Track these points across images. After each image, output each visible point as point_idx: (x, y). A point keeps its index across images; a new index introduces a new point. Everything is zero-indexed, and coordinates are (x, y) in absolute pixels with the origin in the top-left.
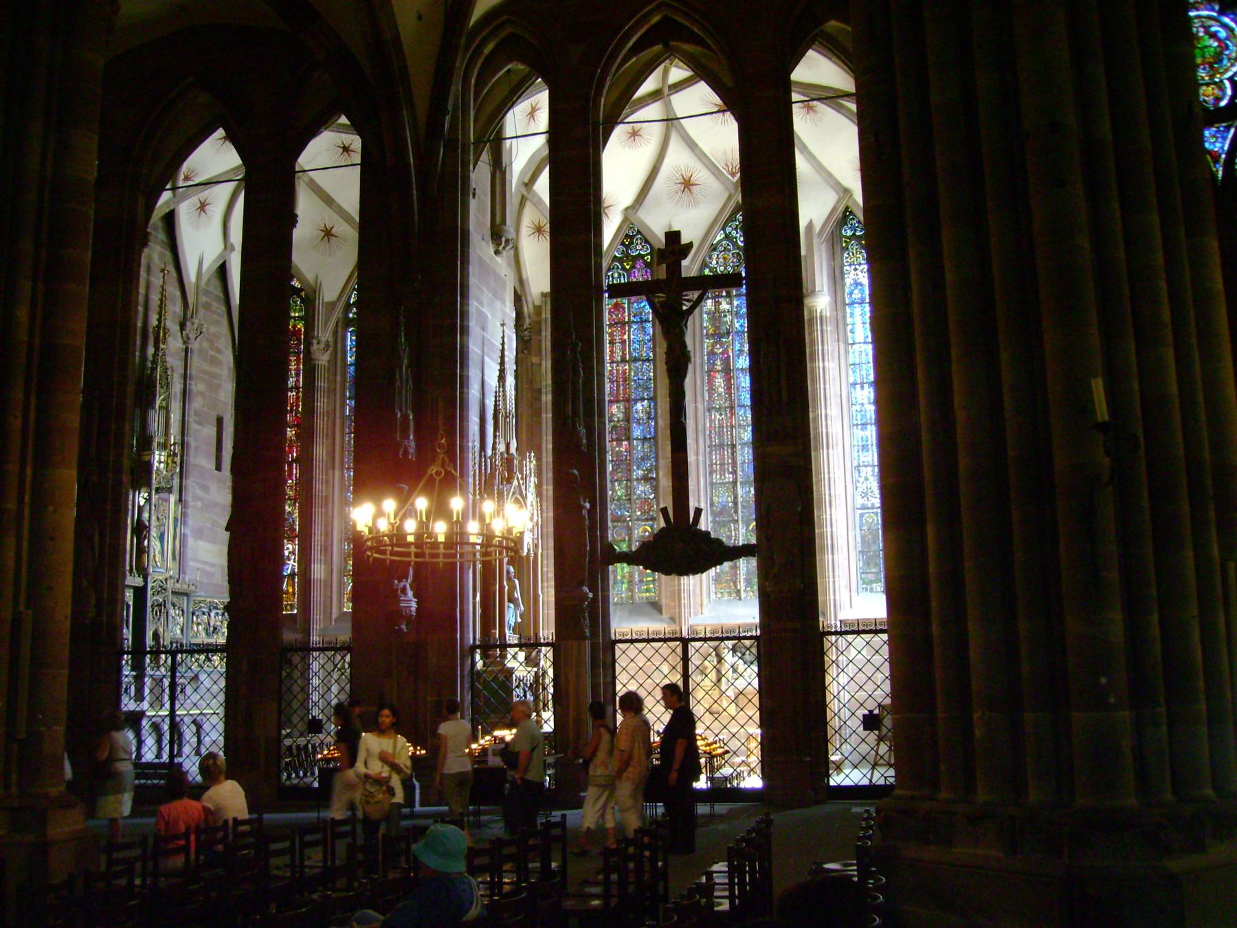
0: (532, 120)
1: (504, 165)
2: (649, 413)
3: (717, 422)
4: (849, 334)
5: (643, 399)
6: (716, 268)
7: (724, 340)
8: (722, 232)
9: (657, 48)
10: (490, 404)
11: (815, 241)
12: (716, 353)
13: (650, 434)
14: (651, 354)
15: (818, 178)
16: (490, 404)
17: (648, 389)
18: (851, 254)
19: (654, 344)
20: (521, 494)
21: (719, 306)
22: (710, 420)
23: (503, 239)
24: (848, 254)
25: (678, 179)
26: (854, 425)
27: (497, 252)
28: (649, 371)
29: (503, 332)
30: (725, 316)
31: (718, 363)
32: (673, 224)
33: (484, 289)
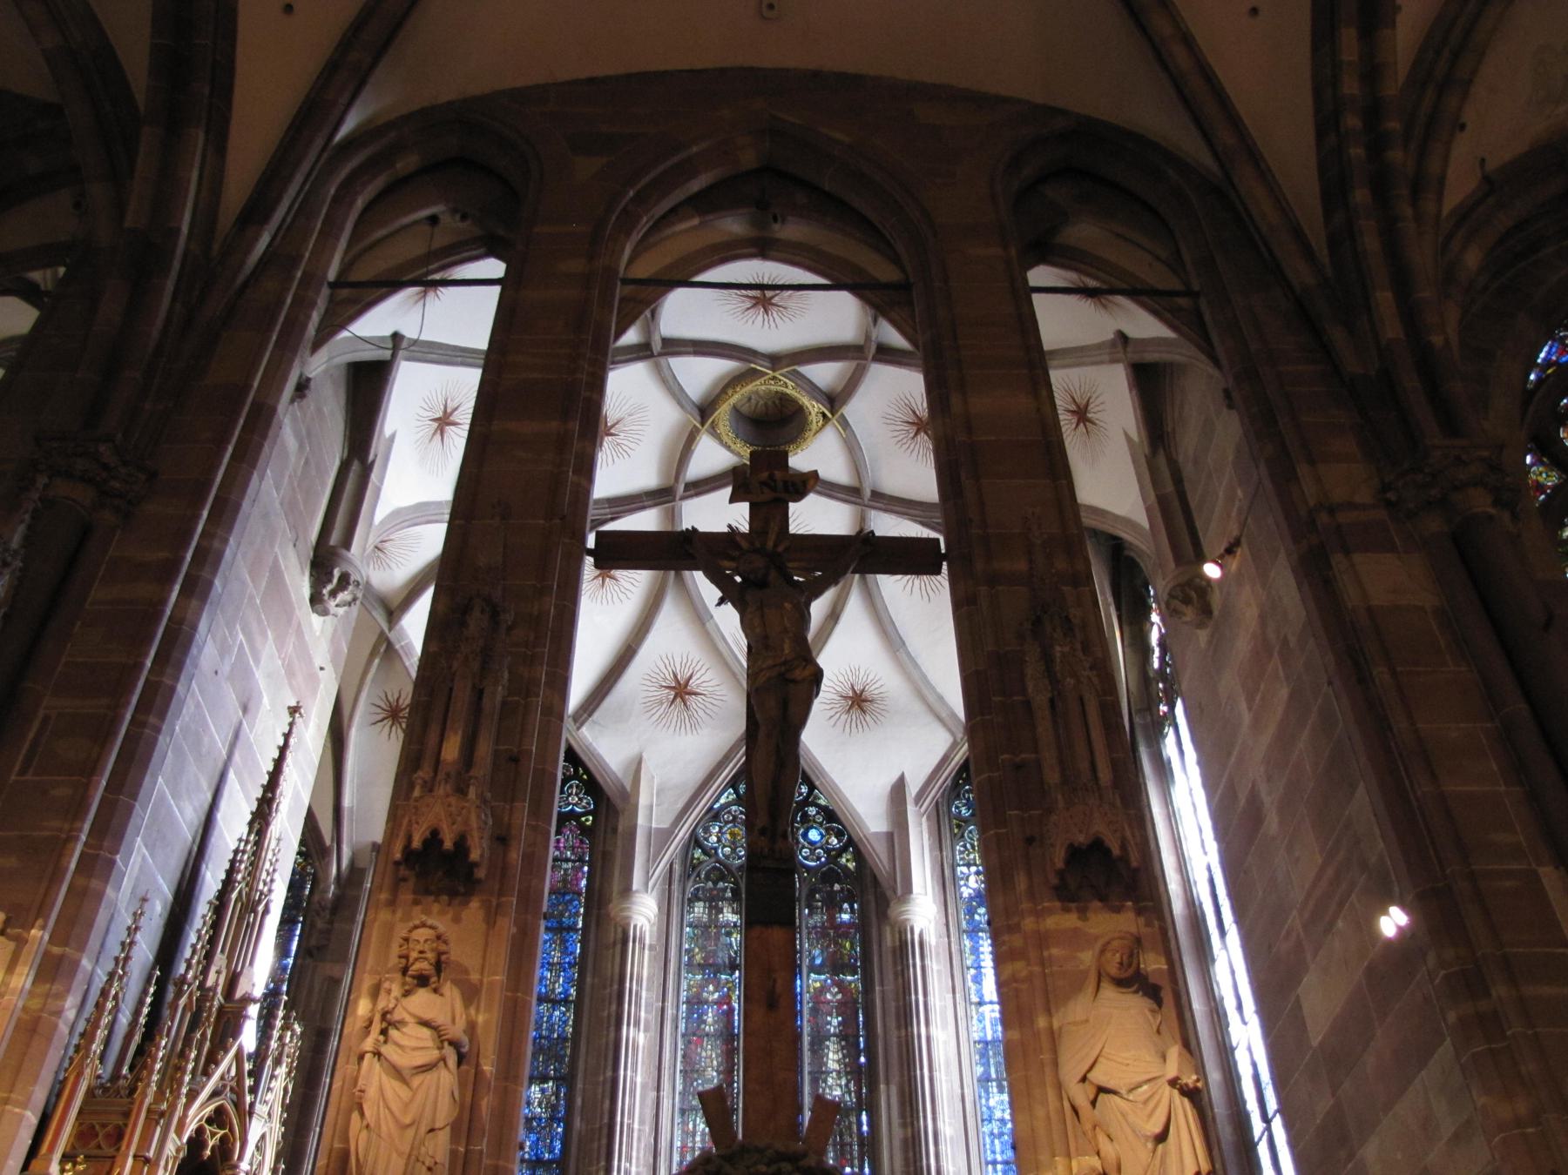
0: (438, 436)
1: (371, 458)
2: (554, 1108)
3: (698, 1138)
4: (970, 983)
5: (544, 1079)
6: (716, 849)
7: (723, 977)
8: (731, 790)
9: (733, 225)
10: (211, 880)
11: (911, 809)
12: (706, 1002)
13: (551, 1151)
14: (572, 991)
15: (918, 707)
16: (211, 880)
17: (559, 1059)
18: (968, 846)
19: (582, 973)
20: (238, 1104)
21: (717, 914)
22: (685, 1133)
23: (337, 573)
24: (965, 846)
25: (665, 679)
26: (987, 1163)
27: (316, 600)
28: (565, 1022)
29: (291, 725)
30: (729, 934)
31: (710, 1018)
32: (645, 756)
33: (269, 633)
